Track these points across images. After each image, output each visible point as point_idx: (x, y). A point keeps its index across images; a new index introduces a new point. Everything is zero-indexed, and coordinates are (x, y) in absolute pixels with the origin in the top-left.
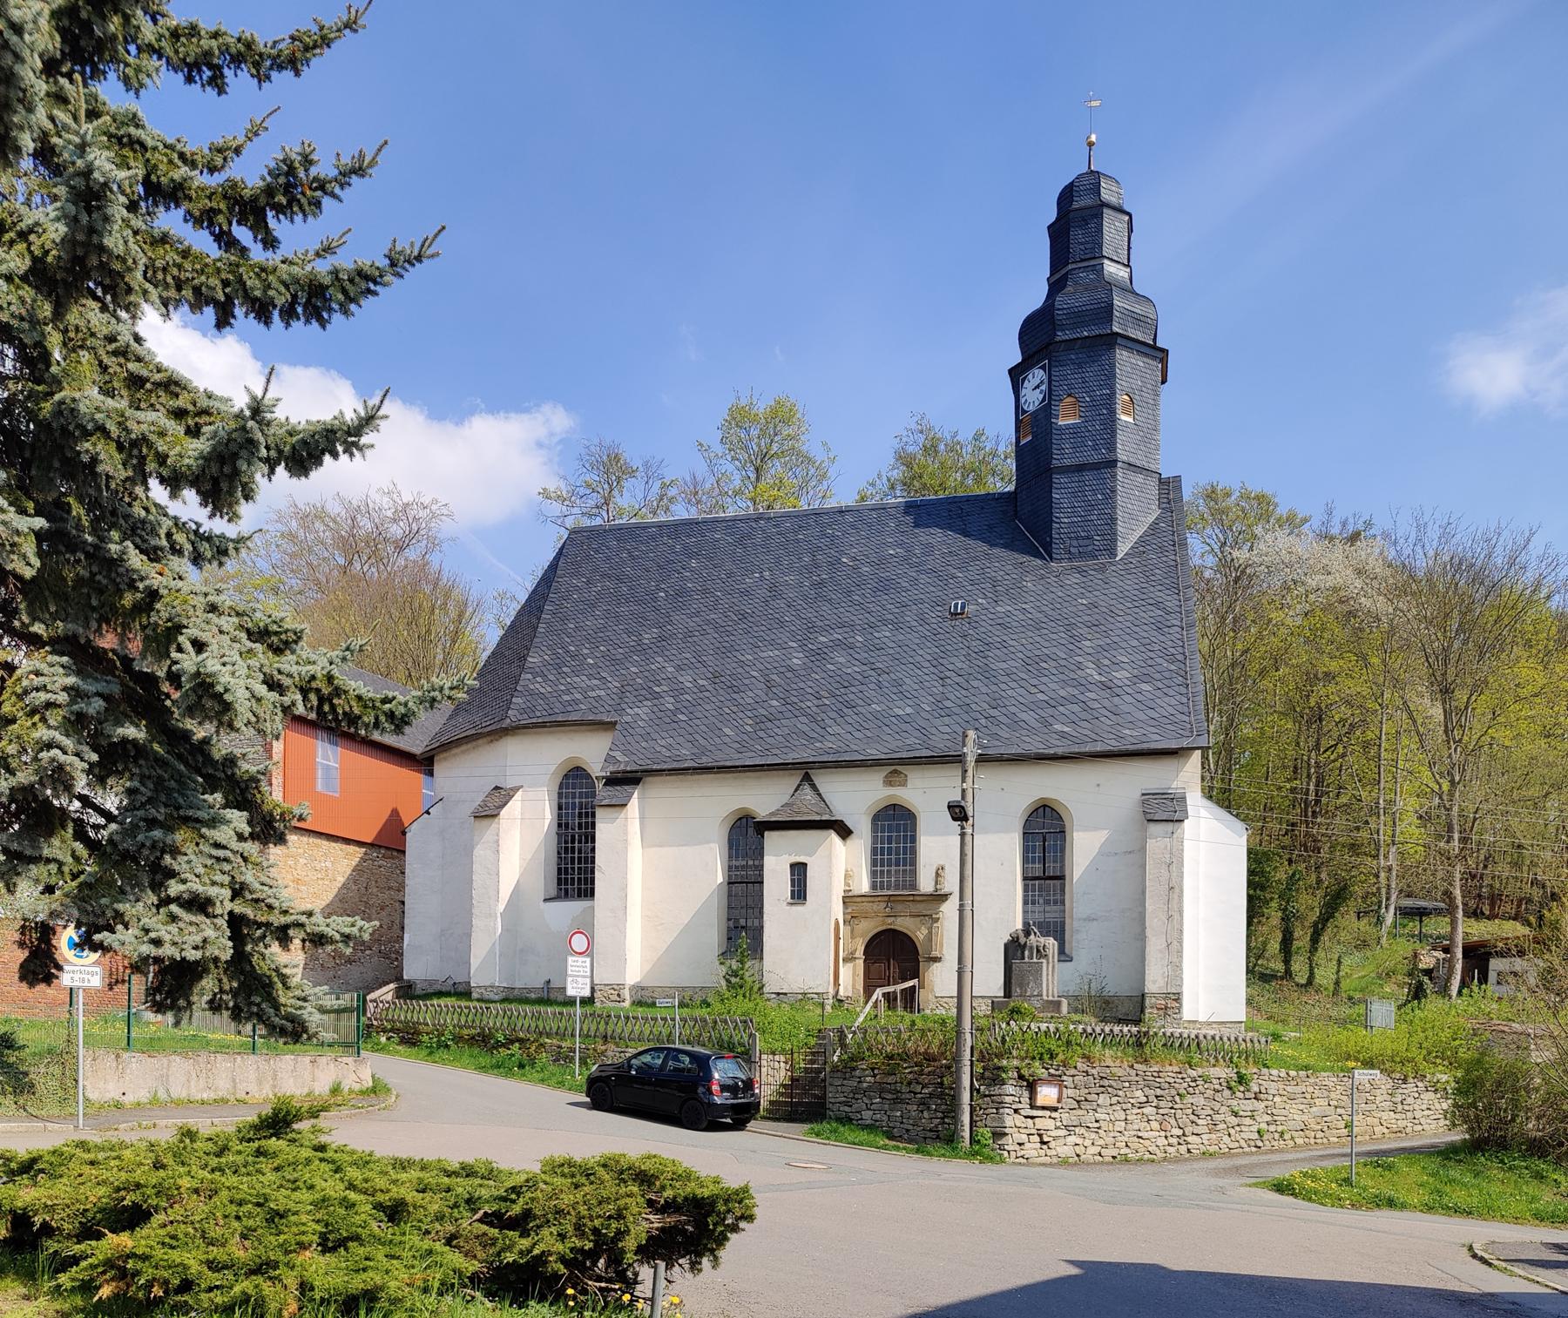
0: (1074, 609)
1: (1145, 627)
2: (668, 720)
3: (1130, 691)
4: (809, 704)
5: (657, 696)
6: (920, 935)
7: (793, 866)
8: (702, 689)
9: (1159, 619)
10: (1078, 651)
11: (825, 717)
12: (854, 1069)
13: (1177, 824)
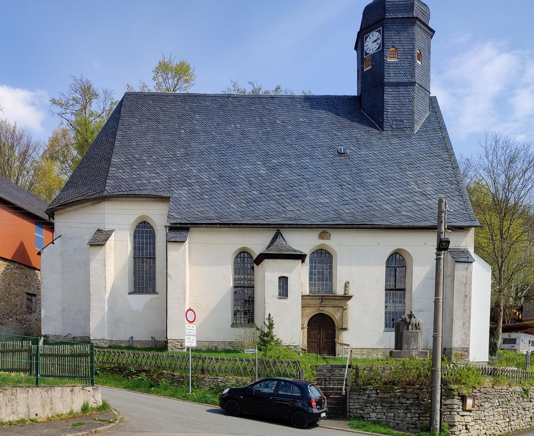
0: (399, 156)
1: (435, 167)
2: (198, 198)
3: (435, 197)
4: (274, 194)
5: (190, 185)
6: (336, 315)
7: (280, 278)
8: (214, 183)
9: (441, 163)
10: (405, 176)
11: (284, 202)
12: (365, 390)
13: (470, 264)
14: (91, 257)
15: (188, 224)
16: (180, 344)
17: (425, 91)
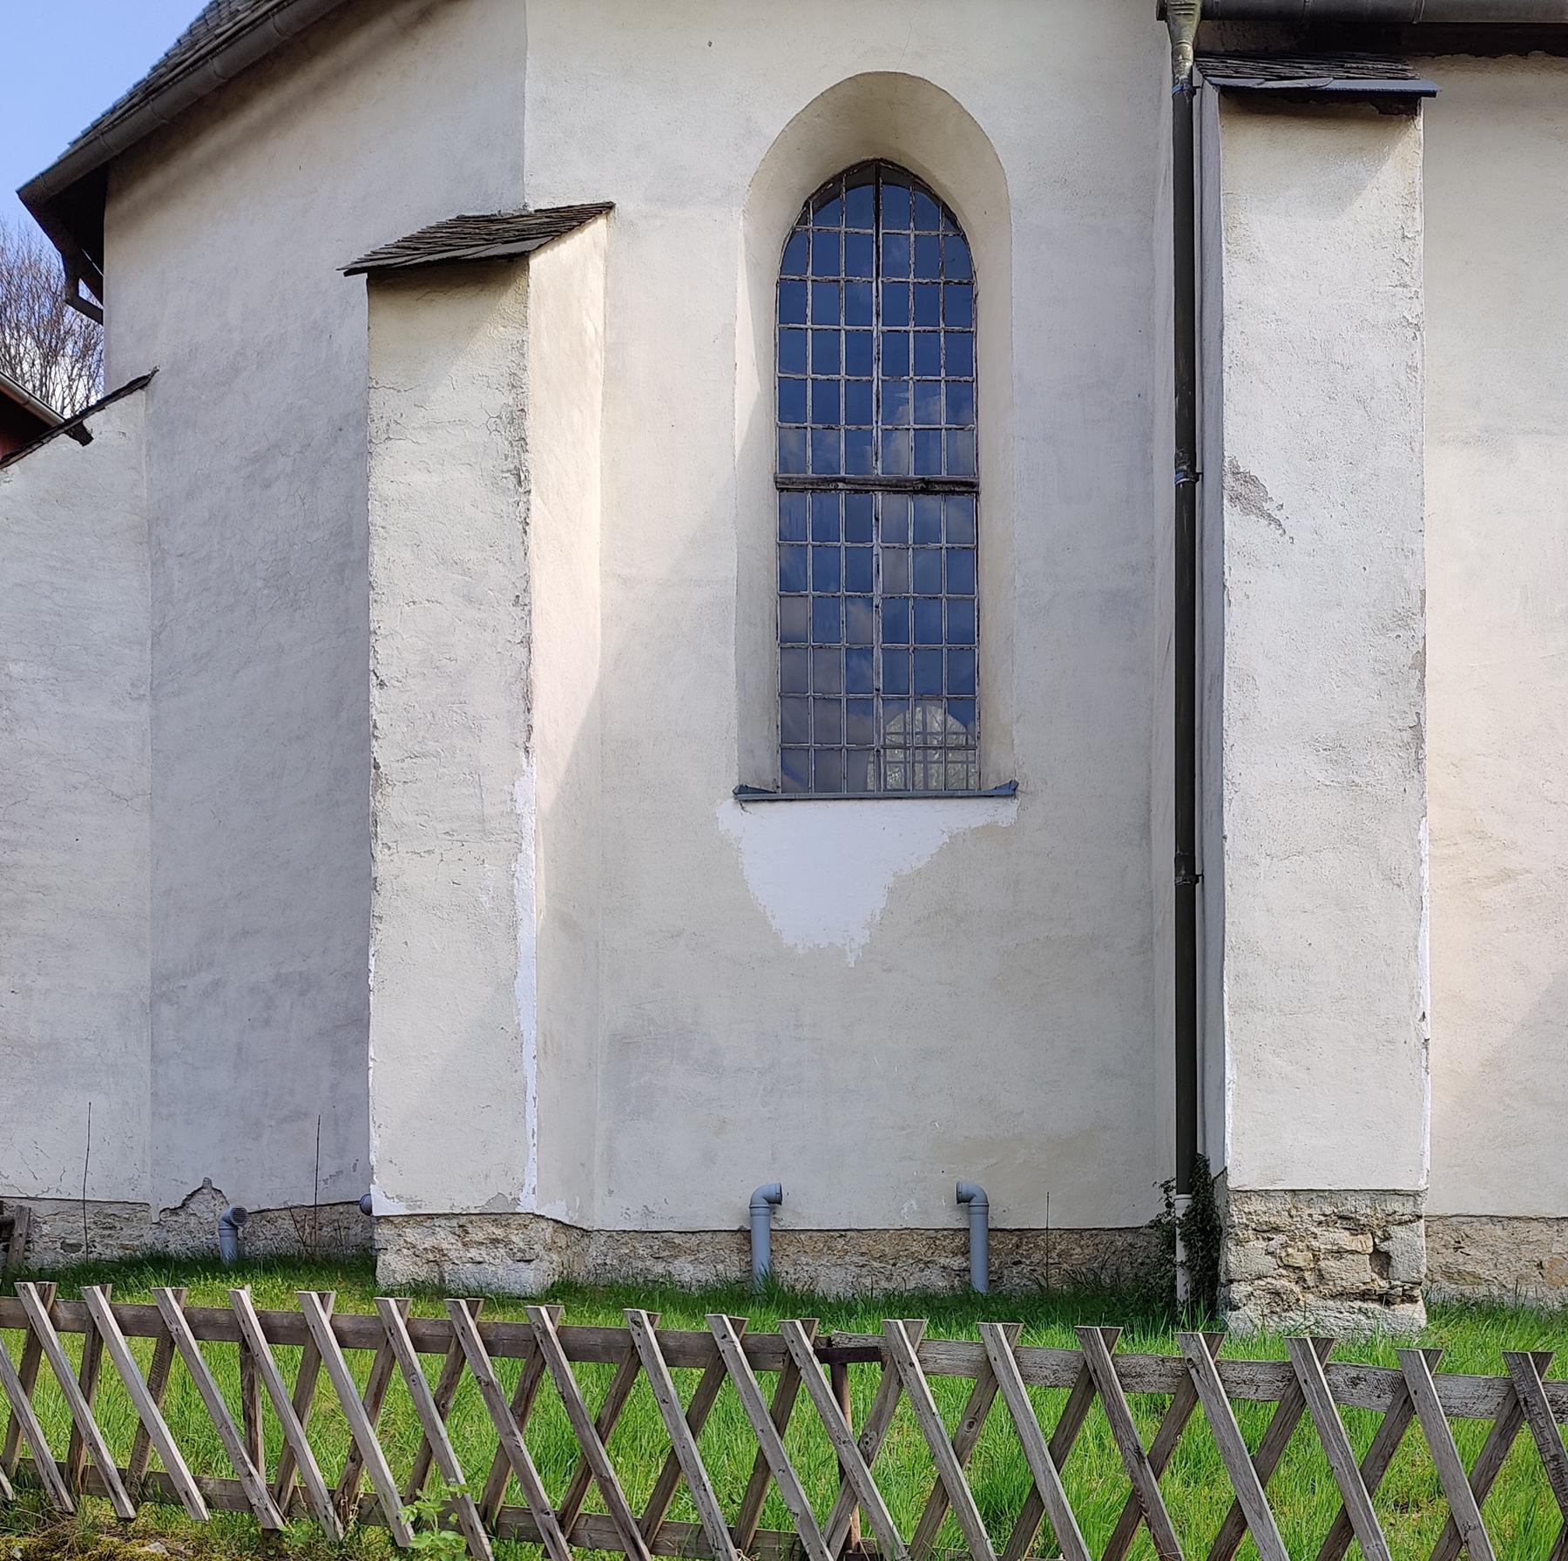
14: (384, 404)
16: (1366, 1243)
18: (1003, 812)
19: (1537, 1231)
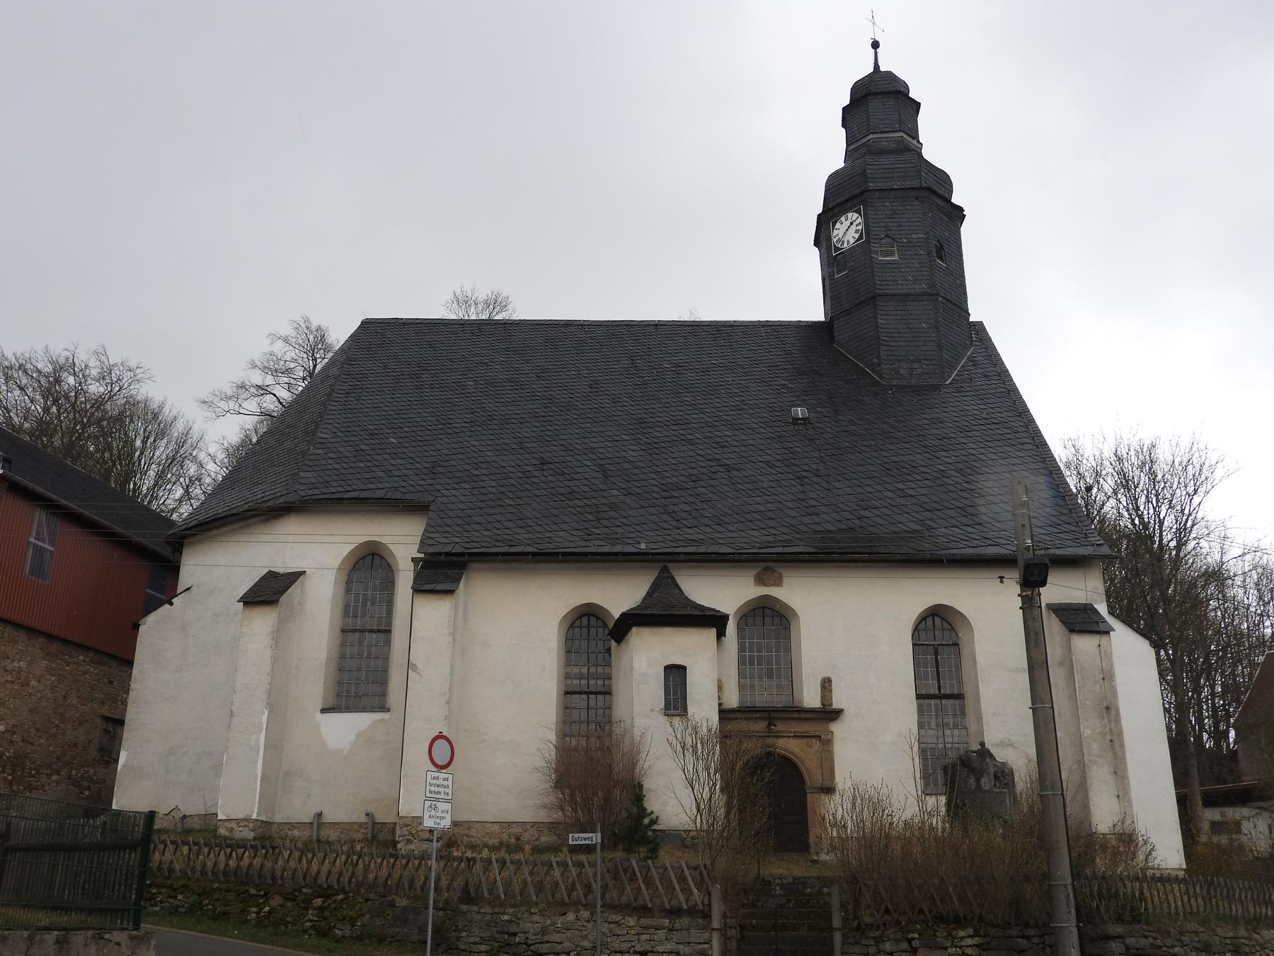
15: (462, 554)
17: (958, 310)
18: (386, 716)
19: (488, 825)
